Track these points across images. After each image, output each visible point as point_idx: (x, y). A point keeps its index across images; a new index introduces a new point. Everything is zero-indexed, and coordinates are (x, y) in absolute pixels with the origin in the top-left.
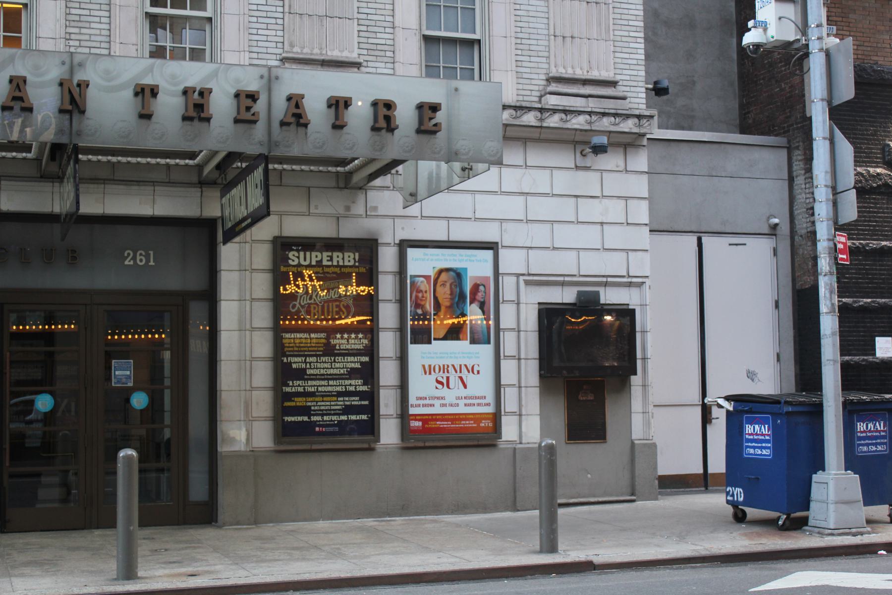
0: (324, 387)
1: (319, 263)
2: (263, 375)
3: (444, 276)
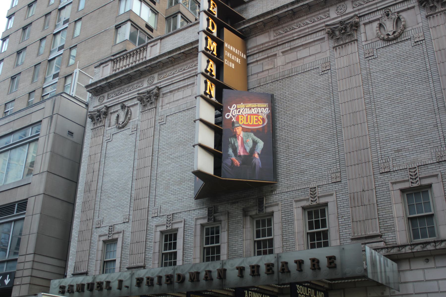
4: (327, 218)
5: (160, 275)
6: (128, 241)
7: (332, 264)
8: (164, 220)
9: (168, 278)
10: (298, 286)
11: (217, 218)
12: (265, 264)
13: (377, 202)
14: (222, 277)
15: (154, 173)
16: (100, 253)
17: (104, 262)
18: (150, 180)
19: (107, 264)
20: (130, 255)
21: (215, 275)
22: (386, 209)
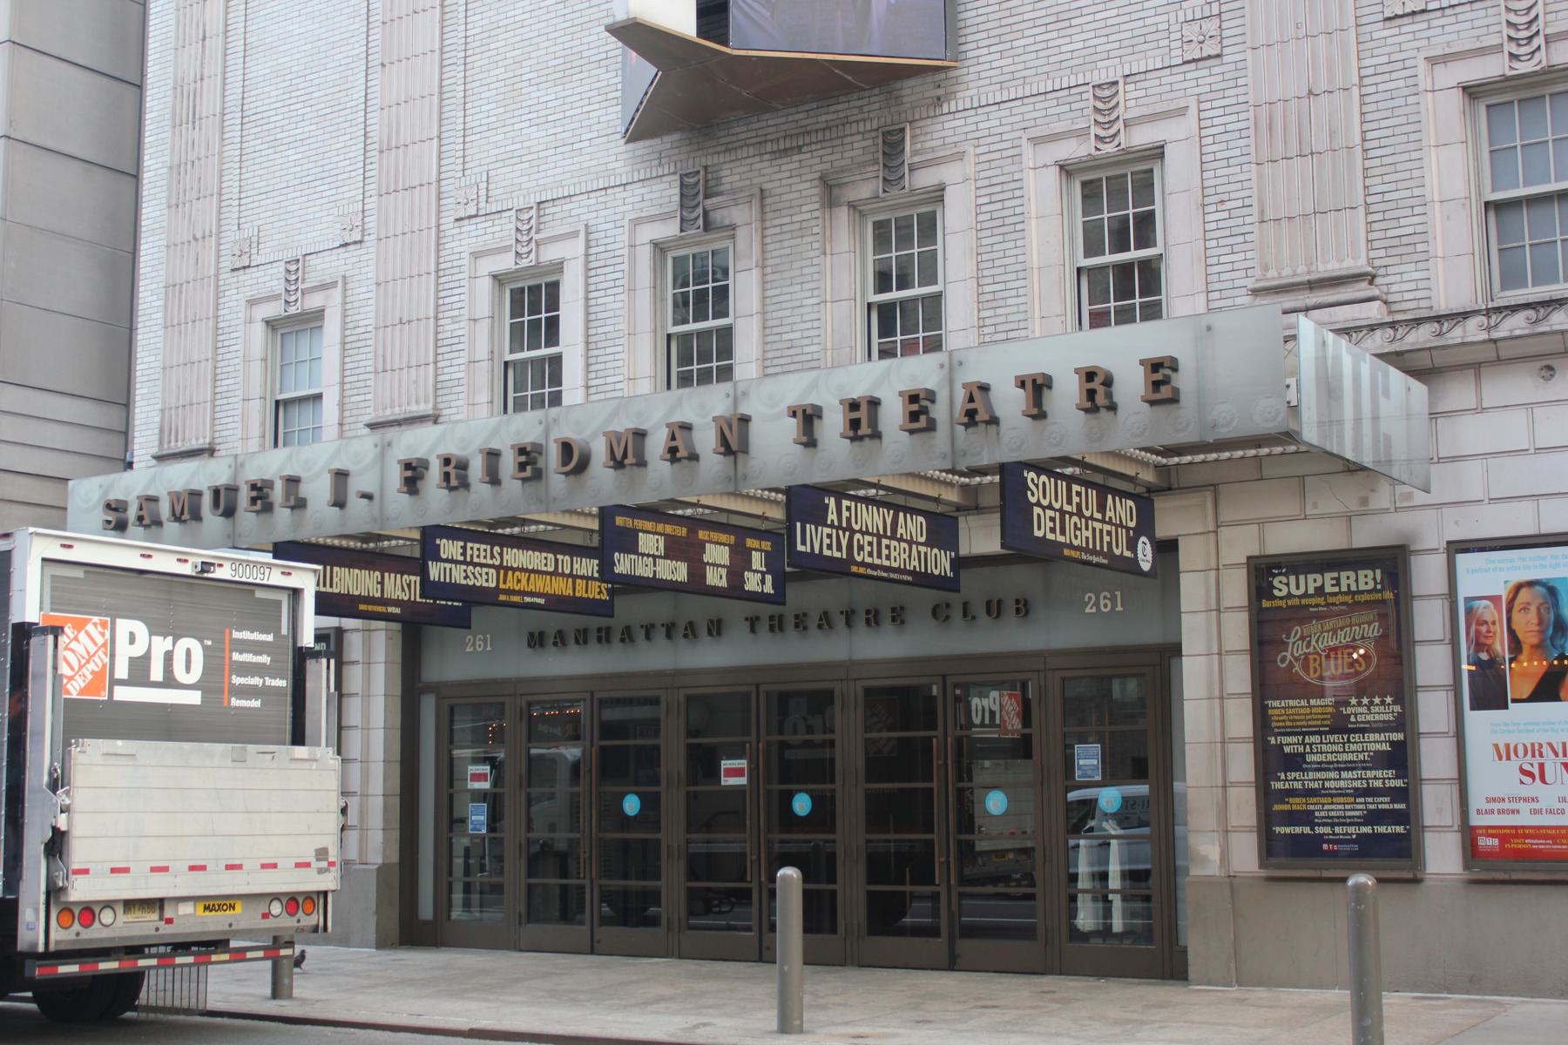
0: (1333, 781)
1: (1320, 591)
2: (1243, 765)
3: (1524, 594)
4: (1158, 207)
5: (495, 445)
6: (366, 317)
7: (1163, 389)
8: (504, 230)
9: (523, 459)
10: (1032, 475)
11: (716, 216)
12: (901, 394)
13: (1364, 140)
14: (734, 447)
15: (455, 37)
16: (256, 369)
17: (277, 403)
18: (442, 67)
19: (287, 413)
20: (376, 372)
21: (706, 440)
22: (1399, 167)
